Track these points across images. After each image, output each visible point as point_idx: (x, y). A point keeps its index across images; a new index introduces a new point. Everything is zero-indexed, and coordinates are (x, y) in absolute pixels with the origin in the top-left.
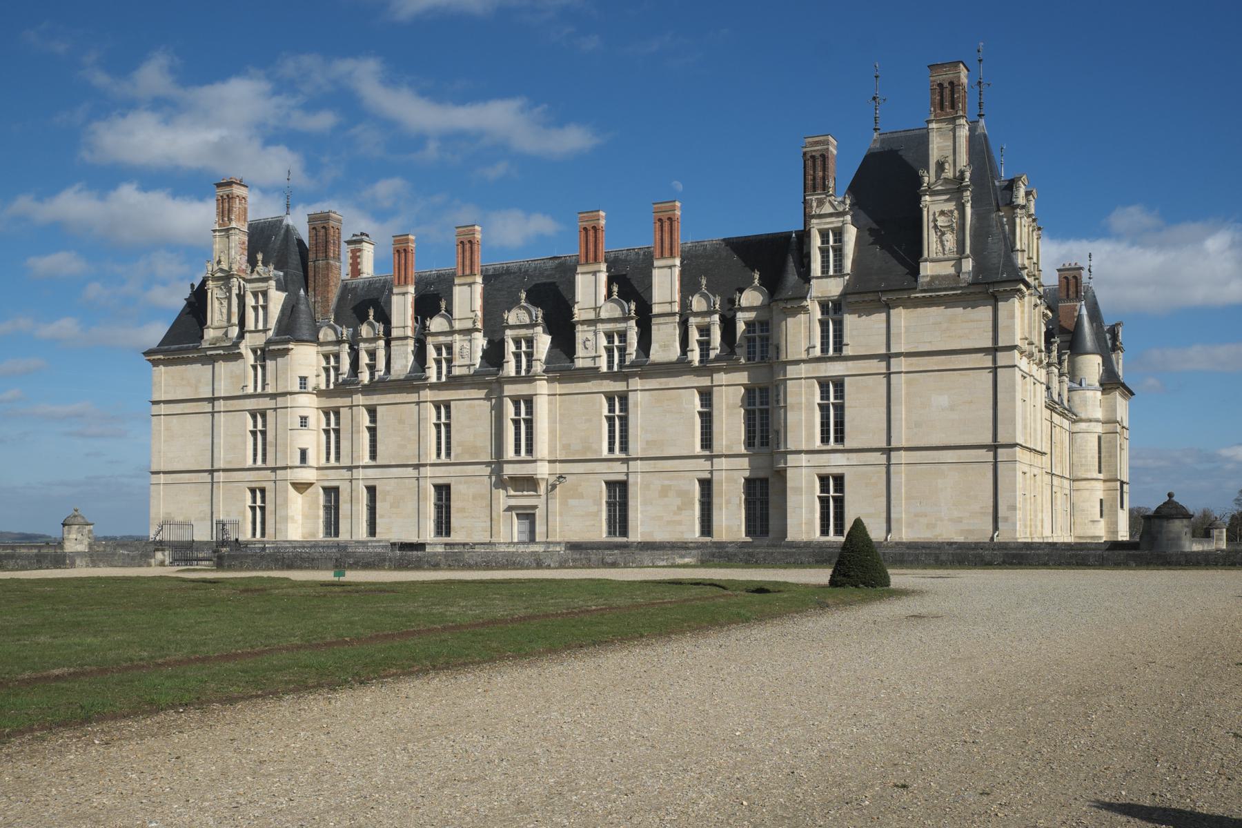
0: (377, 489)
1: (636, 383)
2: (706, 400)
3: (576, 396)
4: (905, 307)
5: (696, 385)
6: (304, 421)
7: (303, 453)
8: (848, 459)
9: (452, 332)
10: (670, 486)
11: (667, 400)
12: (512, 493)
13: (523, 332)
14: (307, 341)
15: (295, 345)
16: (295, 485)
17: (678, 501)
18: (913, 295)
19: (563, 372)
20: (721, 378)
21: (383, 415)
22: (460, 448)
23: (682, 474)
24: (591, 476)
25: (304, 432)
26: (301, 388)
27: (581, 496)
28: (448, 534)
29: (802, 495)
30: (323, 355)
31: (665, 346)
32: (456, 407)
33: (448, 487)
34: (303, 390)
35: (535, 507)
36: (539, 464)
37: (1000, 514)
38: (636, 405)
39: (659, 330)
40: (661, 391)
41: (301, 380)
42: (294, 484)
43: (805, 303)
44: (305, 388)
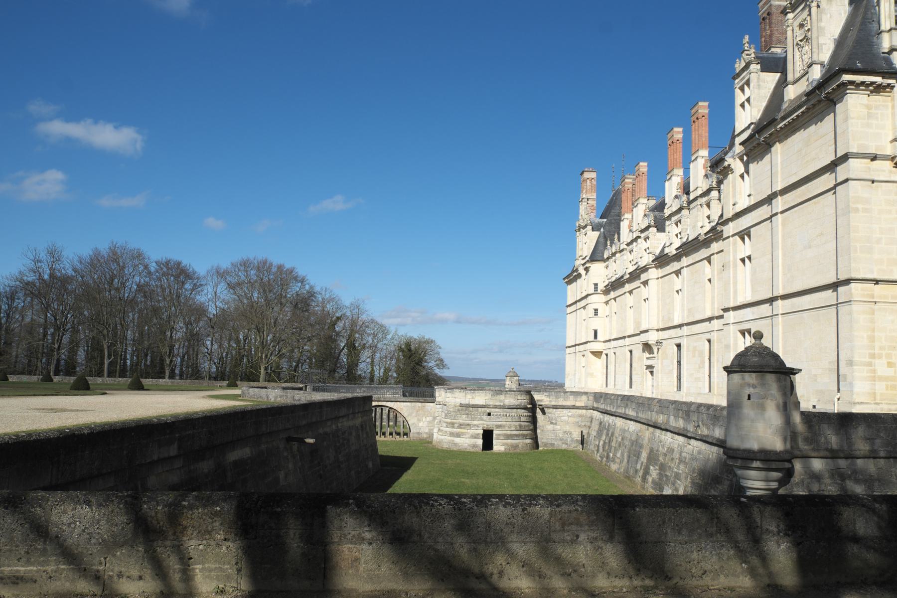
4: (780, 141)
6: (596, 311)
7: (596, 332)
8: (753, 313)
12: (648, 355)
14: (599, 261)
15: (591, 264)
16: (593, 353)
18: (778, 127)
19: (659, 260)
25: (596, 319)
26: (595, 291)
29: (730, 352)
34: (596, 292)
36: (650, 332)
37: (840, 373)
40: (691, 266)
41: (595, 286)
42: (593, 353)
43: (726, 164)
44: (597, 290)
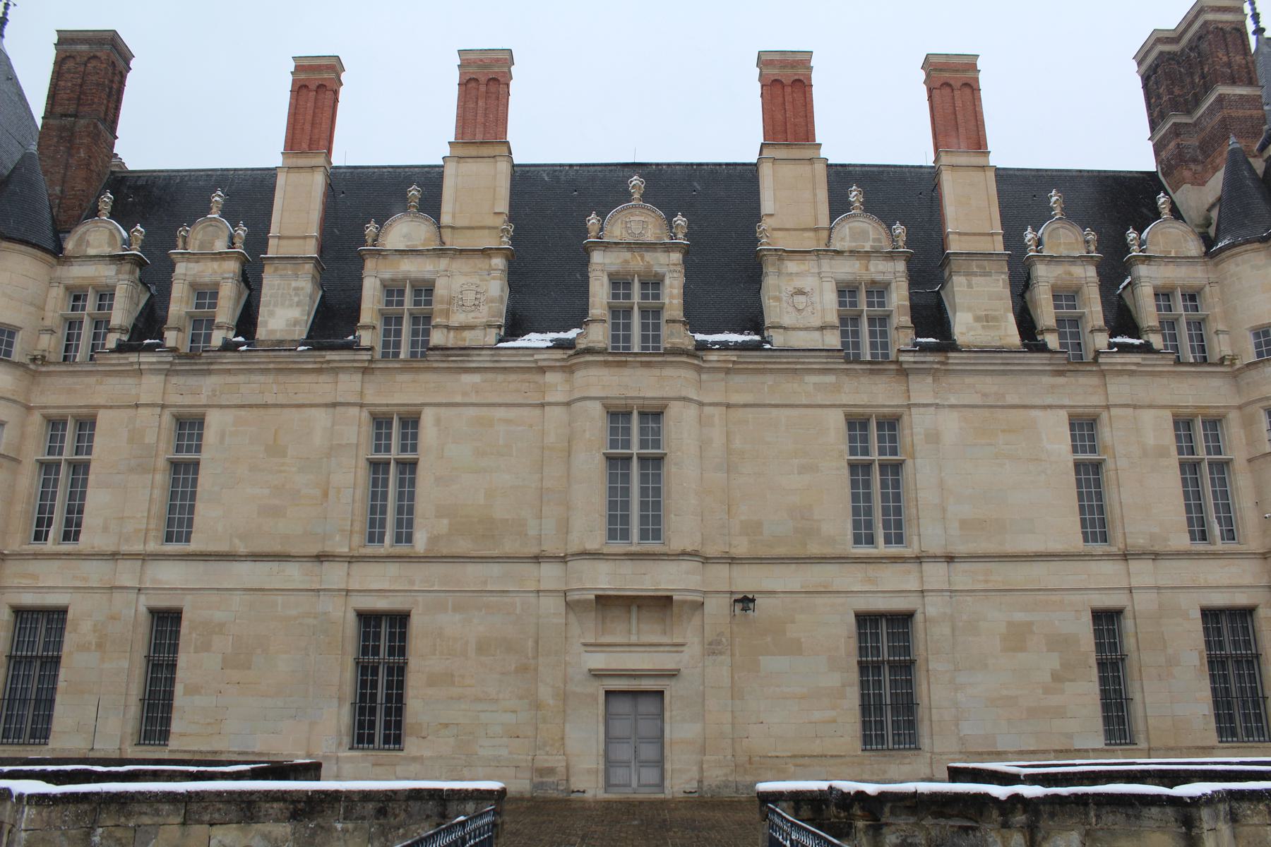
0: (184, 616)
1: (922, 389)
2: (1082, 437)
3: (775, 411)
5: (1066, 402)
9: (441, 252)
10: (1031, 624)
11: (1003, 431)
13: (637, 263)
14: (34, 246)
17: (1053, 662)
20: (1119, 389)
21: (222, 436)
22: (445, 521)
23: (1055, 597)
24: (819, 600)
27: (795, 648)
28: (394, 737)
30: (68, 288)
31: (987, 318)
32: (438, 422)
33: (400, 620)
35: (672, 675)
38: (934, 437)
39: (970, 286)
